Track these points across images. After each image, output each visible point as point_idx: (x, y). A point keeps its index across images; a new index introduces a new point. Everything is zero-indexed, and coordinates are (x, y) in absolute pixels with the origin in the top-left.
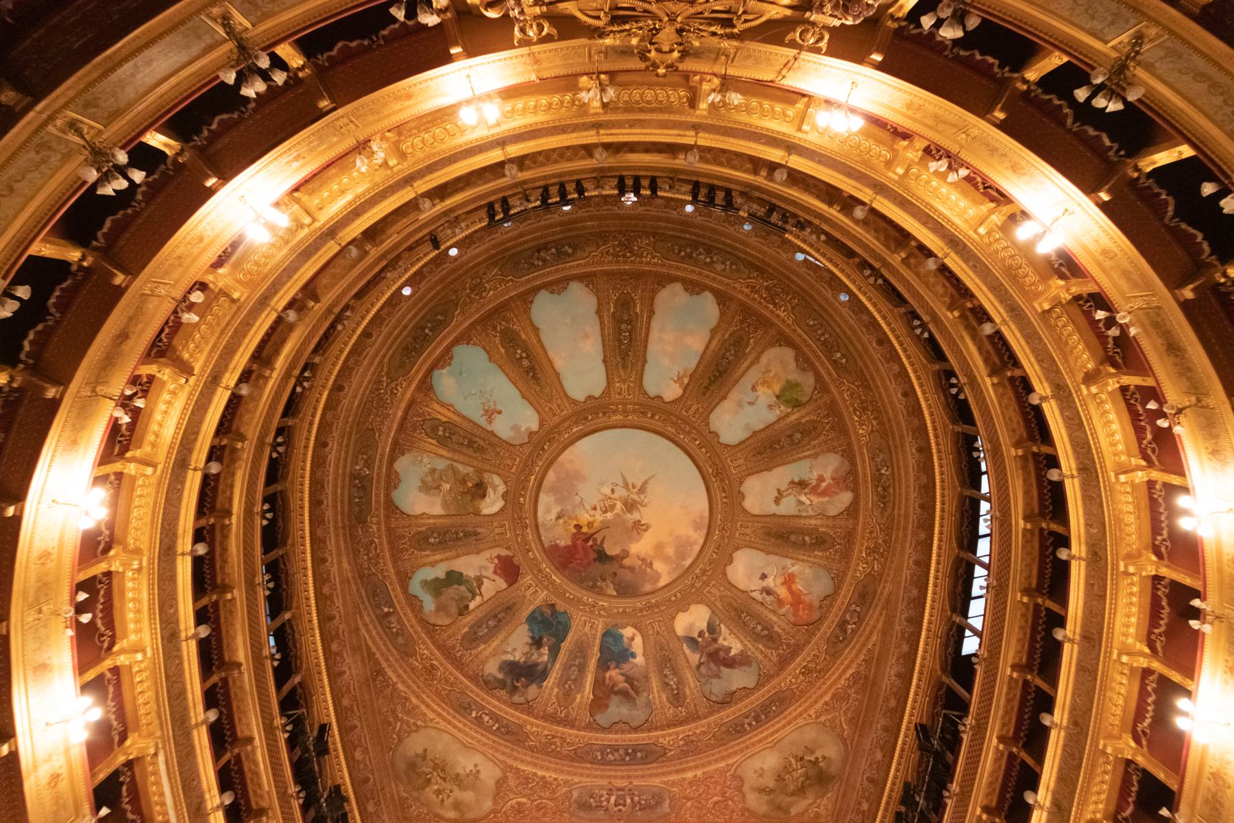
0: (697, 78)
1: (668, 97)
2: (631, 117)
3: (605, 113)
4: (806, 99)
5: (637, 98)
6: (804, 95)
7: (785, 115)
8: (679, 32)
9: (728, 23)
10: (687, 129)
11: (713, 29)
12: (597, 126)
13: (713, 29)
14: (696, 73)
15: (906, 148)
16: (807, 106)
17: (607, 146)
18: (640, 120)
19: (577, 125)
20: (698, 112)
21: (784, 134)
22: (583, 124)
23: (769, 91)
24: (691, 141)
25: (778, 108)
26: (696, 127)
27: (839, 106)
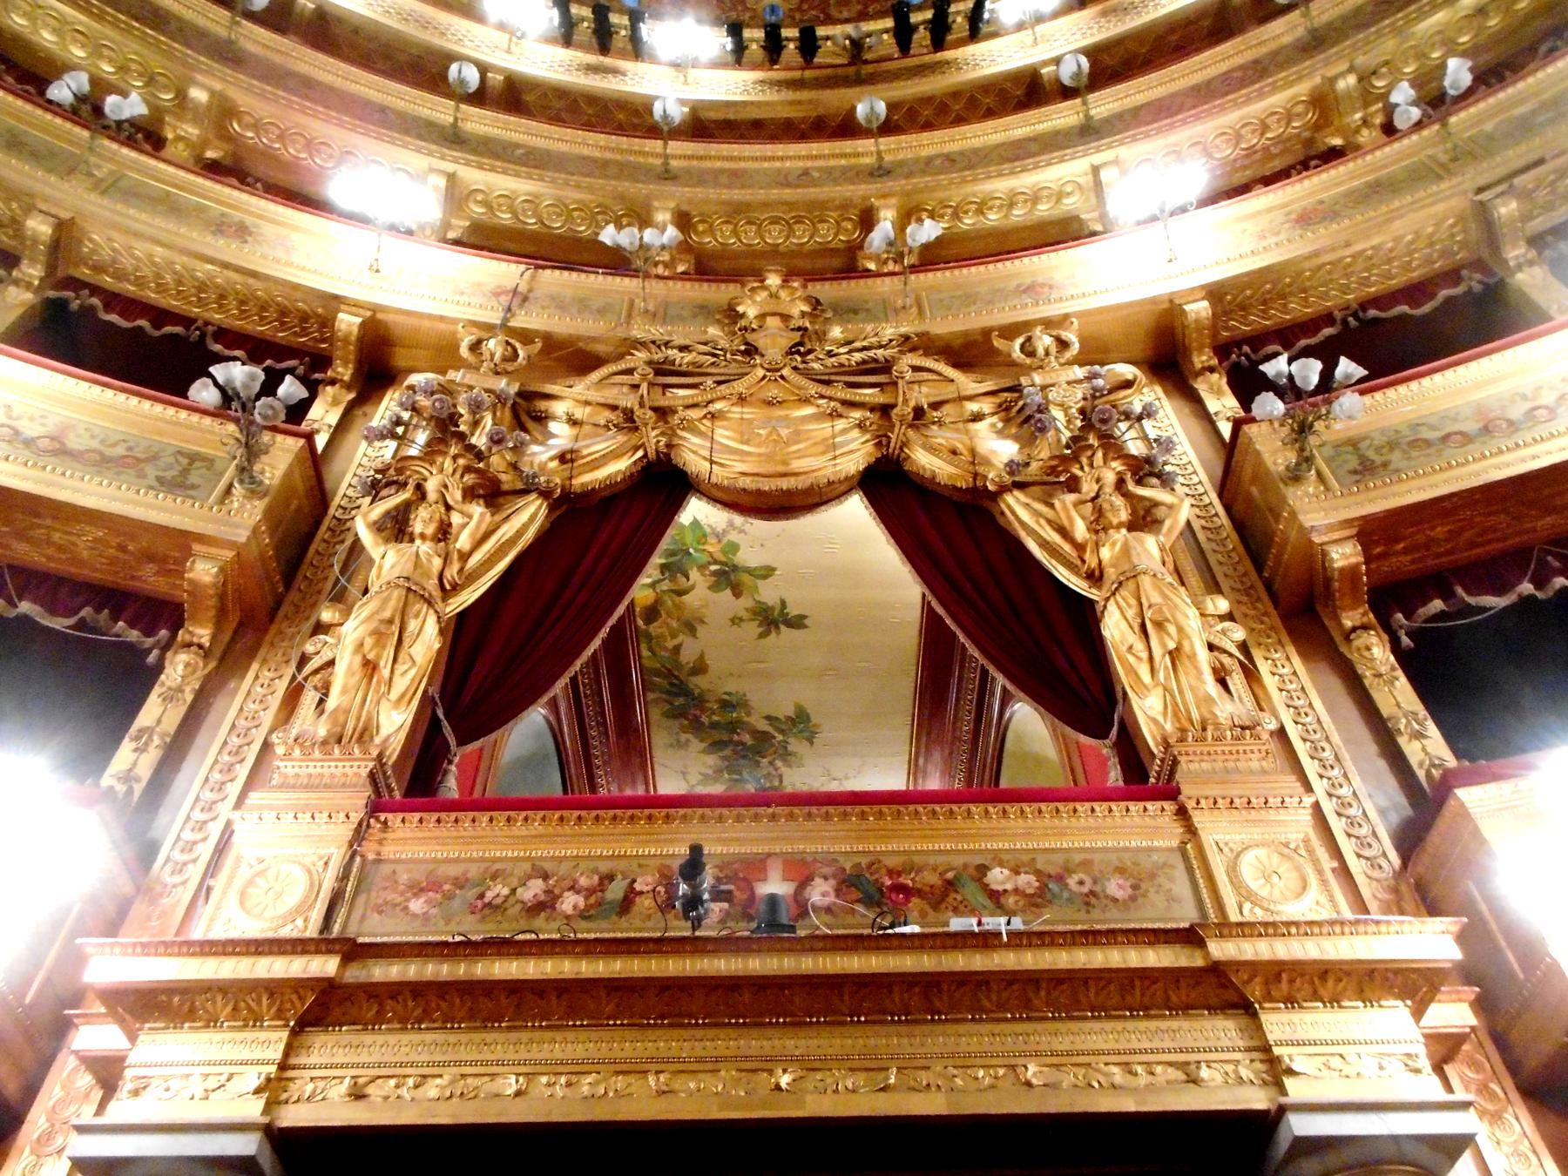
0: (681, 268)
1: (735, 233)
2: (813, 193)
3: (866, 198)
4: (451, 235)
5: (799, 229)
6: (457, 242)
7: (486, 204)
8: (751, 351)
9: (662, 369)
10: (688, 171)
11: (688, 358)
12: (881, 171)
13: (688, 358)
14: (684, 277)
15: (205, 143)
16: (446, 225)
17: (847, 128)
18: (788, 185)
19: (924, 173)
20: (672, 205)
21: (480, 167)
22: (910, 175)
23: (531, 249)
24: (675, 147)
25: (505, 217)
26: (667, 175)
27: (393, 228)
